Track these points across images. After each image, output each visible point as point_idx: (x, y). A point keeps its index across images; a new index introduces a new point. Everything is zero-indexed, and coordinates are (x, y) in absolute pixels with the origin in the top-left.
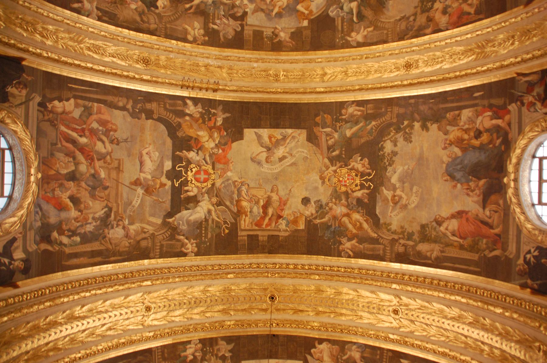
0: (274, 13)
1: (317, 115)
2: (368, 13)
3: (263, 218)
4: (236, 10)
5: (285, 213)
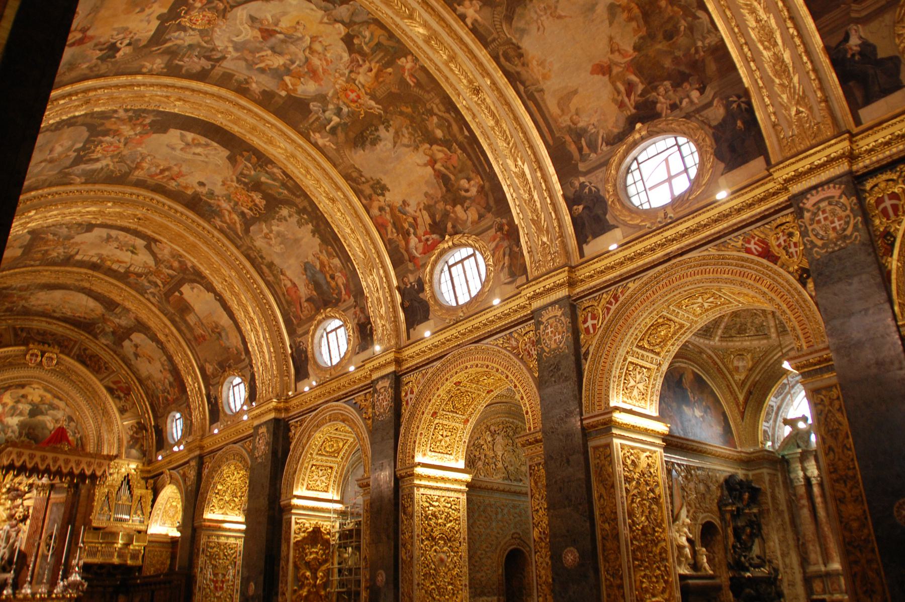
0: (257, 67)
1: (245, 151)
2: (341, 136)
3: (157, 175)
4: (214, 53)
5: (181, 180)
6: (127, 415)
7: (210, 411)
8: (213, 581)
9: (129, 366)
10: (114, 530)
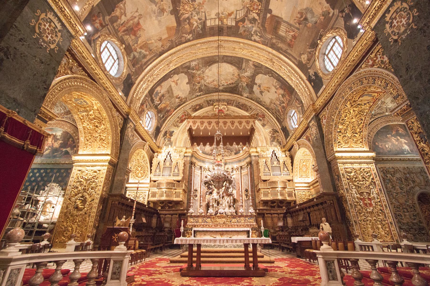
6: (266, 127)
7: (313, 87)
8: (361, 199)
9: (260, 102)
10: (274, 180)
